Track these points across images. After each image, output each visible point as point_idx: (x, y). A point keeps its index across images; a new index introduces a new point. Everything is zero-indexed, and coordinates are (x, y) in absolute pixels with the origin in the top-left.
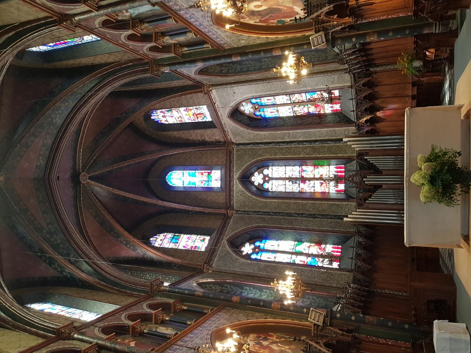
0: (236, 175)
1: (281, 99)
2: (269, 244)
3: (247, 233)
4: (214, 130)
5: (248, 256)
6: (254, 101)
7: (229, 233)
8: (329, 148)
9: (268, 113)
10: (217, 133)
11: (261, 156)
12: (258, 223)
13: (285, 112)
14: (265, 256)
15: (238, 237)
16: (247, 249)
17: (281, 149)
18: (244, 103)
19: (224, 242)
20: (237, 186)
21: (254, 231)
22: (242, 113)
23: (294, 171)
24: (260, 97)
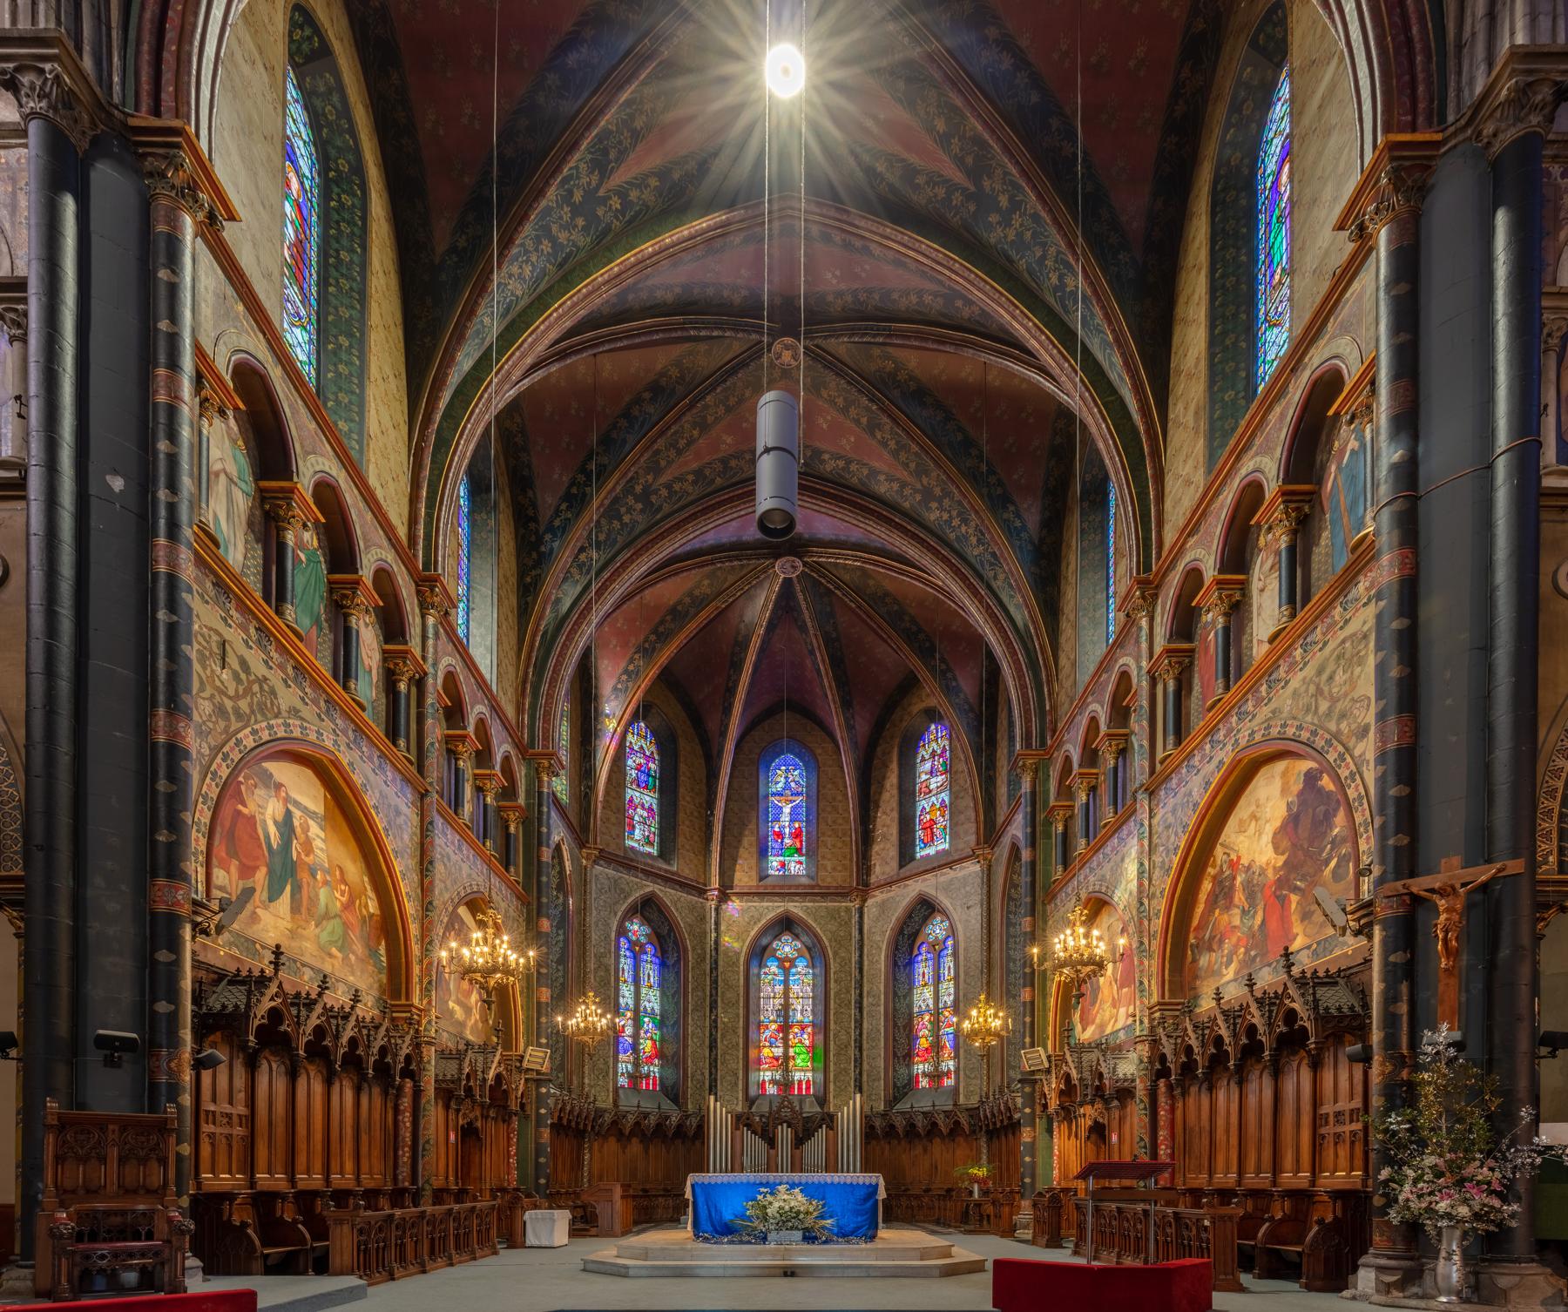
0: (796, 908)
1: (947, 988)
2: (650, 971)
3: (671, 929)
4: (895, 864)
5: (622, 932)
6: (950, 942)
7: (669, 896)
8: (846, 1070)
9: (923, 969)
10: (887, 869)
11: (835, 954)
12: (694, 949)
13: (923, 997)
14: (626, 964)
15: (660, 911)
16: (636, 928)
17: (848, 992)
18: (946, 924)
19: (651, 887)
20: (772, 909)
21: (676, 943)
22: (926, 919)
23: (803, 1010)
24: (955, 955)
